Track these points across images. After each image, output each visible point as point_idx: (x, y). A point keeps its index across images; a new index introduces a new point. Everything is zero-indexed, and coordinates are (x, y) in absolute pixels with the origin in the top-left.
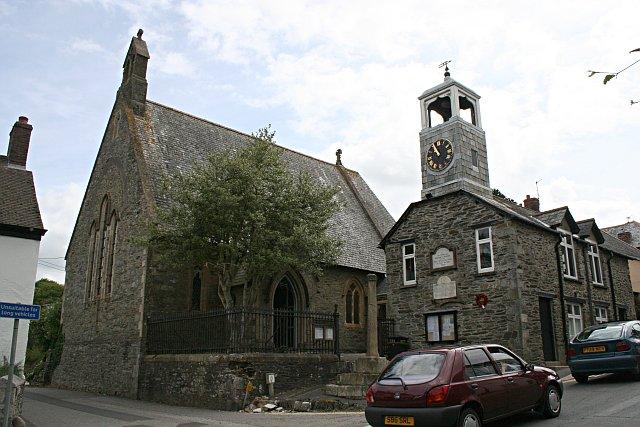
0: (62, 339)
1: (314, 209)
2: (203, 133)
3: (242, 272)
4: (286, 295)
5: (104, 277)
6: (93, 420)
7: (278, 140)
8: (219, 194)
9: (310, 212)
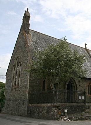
0: (5, 99)
1: (78, 61)
2: (46, 39)
3: (57, 79)
4: (70, 86)
5: (17, 81)
6: (14, 123)
7: (68, 41)
8: (50, 57)
9: (77, 62)
